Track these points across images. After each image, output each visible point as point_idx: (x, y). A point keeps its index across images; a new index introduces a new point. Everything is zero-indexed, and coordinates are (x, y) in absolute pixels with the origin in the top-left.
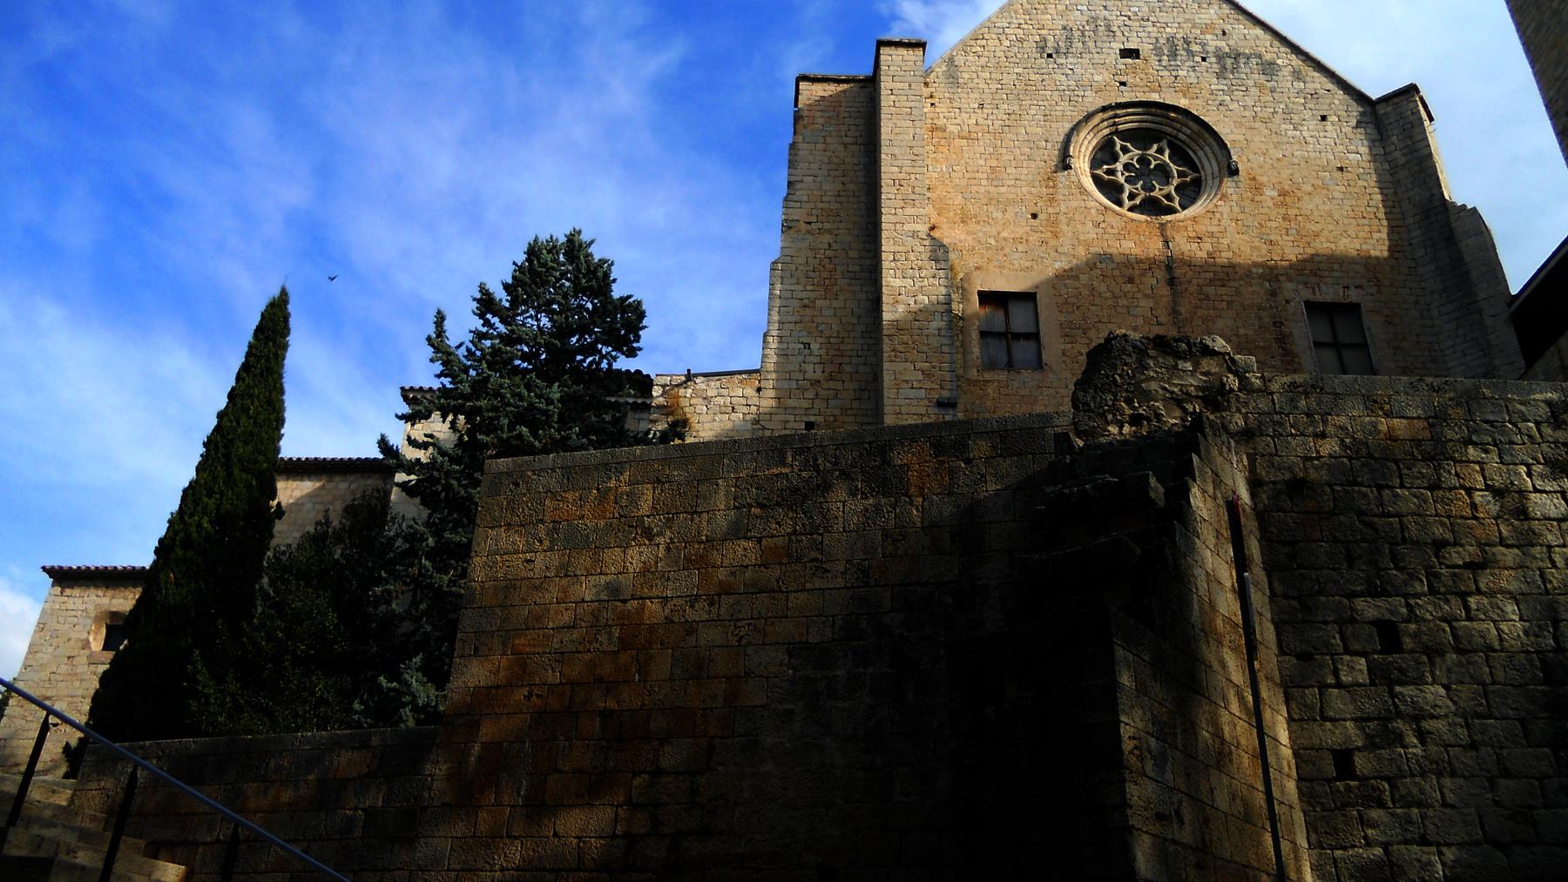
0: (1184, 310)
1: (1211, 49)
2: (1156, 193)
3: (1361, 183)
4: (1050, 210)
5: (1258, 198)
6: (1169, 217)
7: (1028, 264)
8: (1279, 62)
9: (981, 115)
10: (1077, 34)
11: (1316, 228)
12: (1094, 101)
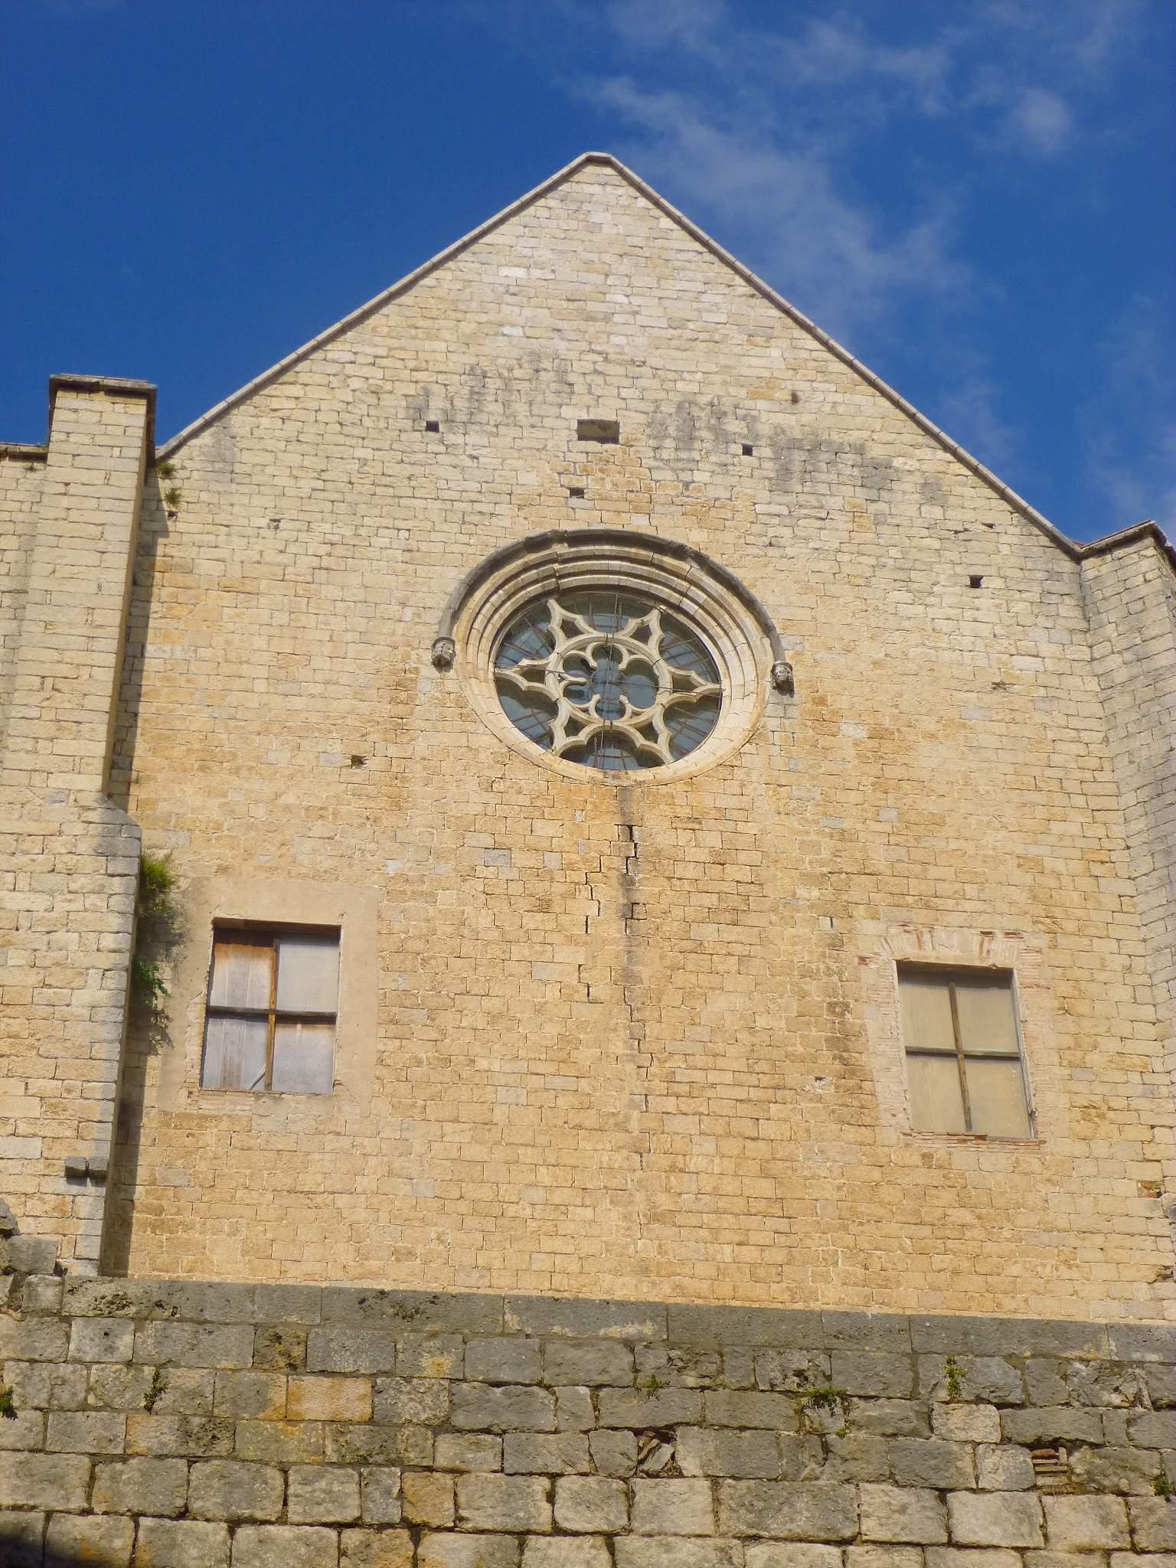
0: (647, 971)
2: (623, 724)
3: (1039, 717)
4: (393, 751)
5: (824, 742)
6: (645, 774)
7: (328, 864)
8: (897, 462)
9: (270, 544)
10: (493, 384)
11: (931, 806)
12: (511, 527)
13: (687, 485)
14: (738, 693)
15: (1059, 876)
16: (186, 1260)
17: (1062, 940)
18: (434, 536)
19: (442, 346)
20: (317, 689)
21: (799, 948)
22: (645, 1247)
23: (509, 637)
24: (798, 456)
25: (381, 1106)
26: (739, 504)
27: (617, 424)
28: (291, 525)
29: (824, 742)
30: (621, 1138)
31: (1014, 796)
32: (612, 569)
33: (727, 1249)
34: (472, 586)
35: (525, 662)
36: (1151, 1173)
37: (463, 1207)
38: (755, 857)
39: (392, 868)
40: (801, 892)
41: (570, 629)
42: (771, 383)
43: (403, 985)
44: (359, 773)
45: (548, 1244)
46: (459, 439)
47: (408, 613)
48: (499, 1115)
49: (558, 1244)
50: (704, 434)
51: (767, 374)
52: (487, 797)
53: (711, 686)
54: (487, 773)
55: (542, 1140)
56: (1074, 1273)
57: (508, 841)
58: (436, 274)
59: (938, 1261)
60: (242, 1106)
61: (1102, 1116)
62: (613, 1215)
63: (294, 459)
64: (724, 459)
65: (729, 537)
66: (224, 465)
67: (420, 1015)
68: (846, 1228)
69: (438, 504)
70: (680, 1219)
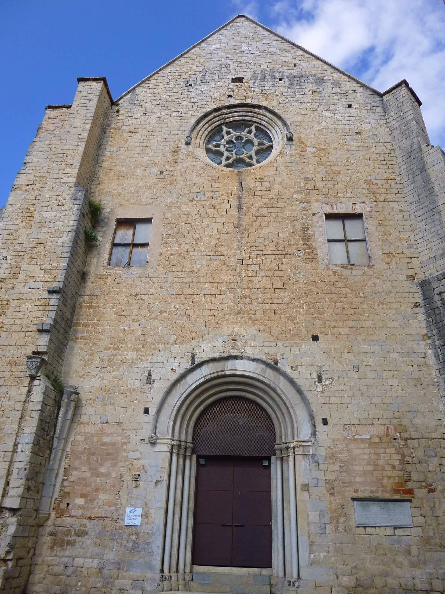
1: (286, 74)
3: (370, 140)
4: (172, 169)
5: (302, 154)
7: (150, 201)
8: (325, 78)
9: (143, 120)
11: (336, 168)
13: (262, 90)
14: (277, 144)
15: (378, 185)
16: (98, 317)
17: (379, 203)
18: (188, 112)
19: (195, 65)
20: (151, 155)
21: (293, 212)
22: (240, 306)
23: (210, 137)
24: (296, 80)
25: (160, 268)
26: (278, 94)
27: (243, 78)
28: (149, 114)
29: (302, 154)
30: (234, 273)
31: (363, 163)
32: (240, 115)
33: (267, 305)
34: (198, 123)
35: (215, 143)
36: (411, 273)
37: (182, 297)
38: (280, 188)
39: (169, 200)
40: (294, 196)
41: (228, 133)
42: (289, 62)
43: (169, 232)
44: (162, 175)
45: (209, 307)
46: (198, 87)
47: (180, 132)
48: (196, 269)
49: (211, 307)
50: (268, 77)
51: (287, 60)
52: (198, 178)
53: (269, 144)
54: (199, 172)
55: (209, 275)
56: (385, 306)
57: (204, 190)
58: (195, 49)
59: (338, 305)
60: (118, 271)
61: (394, 256)
62: (230, 297)
63: (152, 98)
64: (274, 83)
65: (275, 102)
66: (133, 102)
67: (174, 241)
68: (307, 296)
69: (191, 104)
70: (252, 297)
